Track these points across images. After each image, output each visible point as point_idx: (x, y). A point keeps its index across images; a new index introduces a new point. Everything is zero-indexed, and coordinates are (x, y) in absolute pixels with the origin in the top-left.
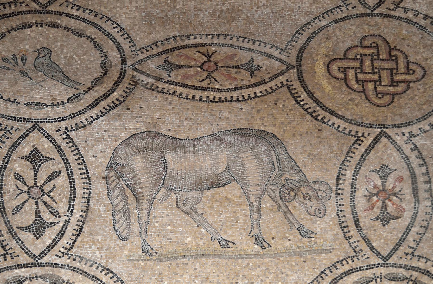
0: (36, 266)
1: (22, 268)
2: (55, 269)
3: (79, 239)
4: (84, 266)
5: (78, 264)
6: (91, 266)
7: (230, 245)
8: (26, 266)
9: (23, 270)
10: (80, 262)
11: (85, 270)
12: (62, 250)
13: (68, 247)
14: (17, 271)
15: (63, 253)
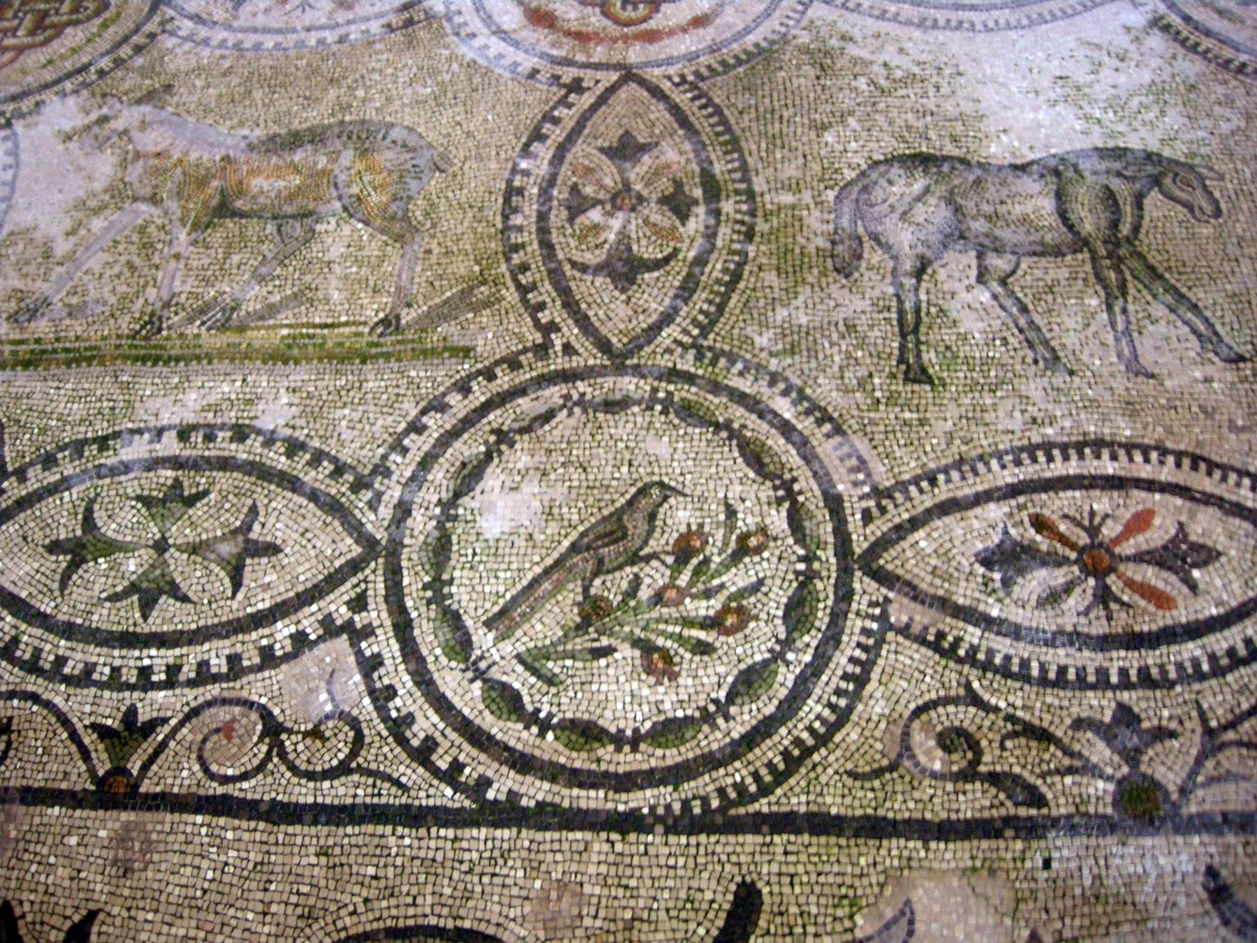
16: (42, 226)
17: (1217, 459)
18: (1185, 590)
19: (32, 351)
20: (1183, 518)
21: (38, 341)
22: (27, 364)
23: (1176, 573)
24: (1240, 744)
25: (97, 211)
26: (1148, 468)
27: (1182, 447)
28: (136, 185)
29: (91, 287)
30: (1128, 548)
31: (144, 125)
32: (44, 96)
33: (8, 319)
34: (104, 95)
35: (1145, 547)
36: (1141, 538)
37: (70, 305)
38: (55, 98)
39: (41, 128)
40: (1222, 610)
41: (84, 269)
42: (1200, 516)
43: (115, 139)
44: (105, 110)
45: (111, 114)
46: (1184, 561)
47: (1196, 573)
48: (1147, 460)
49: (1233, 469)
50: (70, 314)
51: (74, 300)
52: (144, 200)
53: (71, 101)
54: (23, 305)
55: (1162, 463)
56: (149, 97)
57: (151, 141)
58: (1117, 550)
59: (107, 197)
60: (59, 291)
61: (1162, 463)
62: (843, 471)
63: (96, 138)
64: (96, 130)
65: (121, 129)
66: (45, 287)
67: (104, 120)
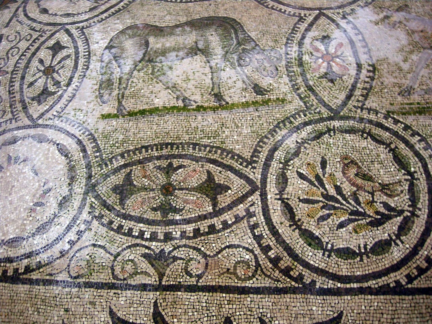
0: (31, 128)
1: (20, 129)
2: (45, 129)
3: (70, 104)
4: (68, 126)
5: (64, 124)
6: (73, 126)
7: (193, 103)
8: (24, 127)
9: (21, 131)
10: (66, 122)
11: (68, 130)
12: (55, 113)
13: (60, 110)
14: (15, 132)
15: (55, 116)
16: (390, 58)
19: (419, 108)
21: (418, 103)
22: (420, 113)
25: (411, 52)
28: (421, 43)
29: (428, 82)
31: (407, 20)
32: (353, 7)
33: (399, 94)
34: (380, 8)
37: (424, 90)
38: (359, 8)
39: (360, 19)
41: (421, 75)
43: (398, 25)
44: (385, 13)
45: (388, 15)
50: (426, 93)
51: (424, 87)
52: (428, 49)
53: (367, 9)
54: (401, 89)
56: (399, 9)
57: (414, 25)
59: (411, 47)
60: (415, 84)
63: (389, 24)
64: (386, 21)
65: (398, 21)
66: (408, 82)
67: (387, 17)
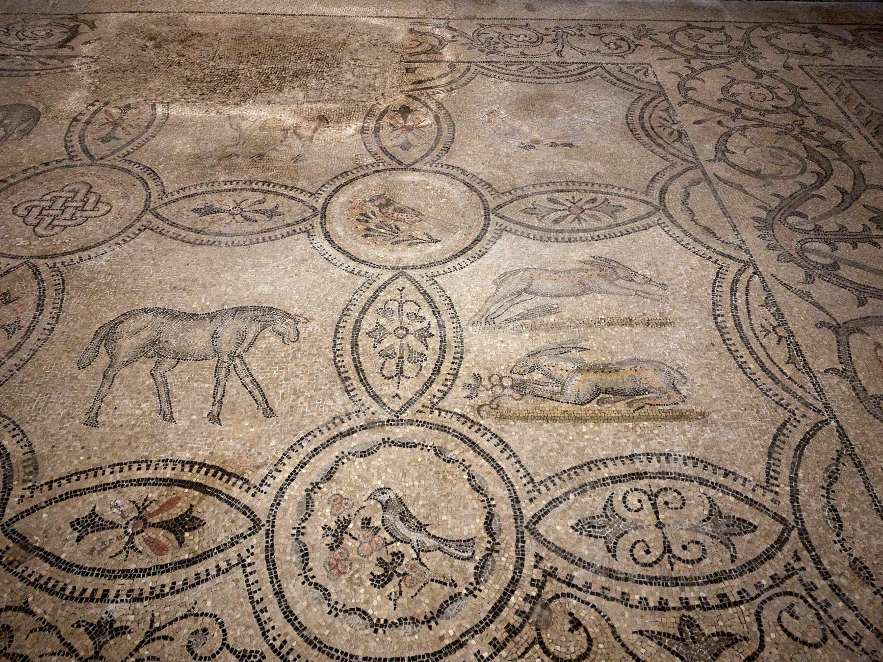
17: (229, 470)
18: (176, 543)
20: (194, 503)
23: (175, 535)
24: (165, 638)
26: (190, 474)
27: (214, 463)
30: (156, 520)
35: (165, 519)
36: (165, 514)
40: (191, 556)
42: (204, 502)
46: (183, 527)
47: (187, 534)
48: (191, 470)
49: (235, 475)
55: (198, 472)
58: (150, 520)
61: (198, 472)
62: (22, 474)
